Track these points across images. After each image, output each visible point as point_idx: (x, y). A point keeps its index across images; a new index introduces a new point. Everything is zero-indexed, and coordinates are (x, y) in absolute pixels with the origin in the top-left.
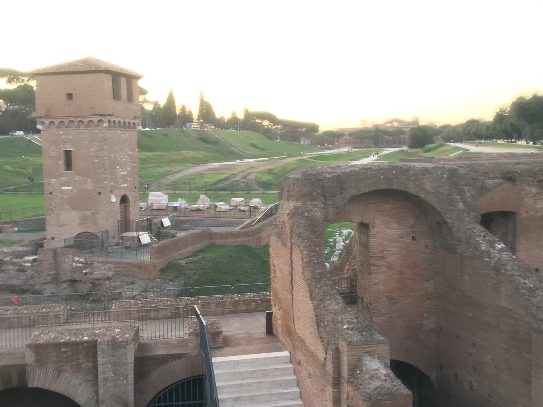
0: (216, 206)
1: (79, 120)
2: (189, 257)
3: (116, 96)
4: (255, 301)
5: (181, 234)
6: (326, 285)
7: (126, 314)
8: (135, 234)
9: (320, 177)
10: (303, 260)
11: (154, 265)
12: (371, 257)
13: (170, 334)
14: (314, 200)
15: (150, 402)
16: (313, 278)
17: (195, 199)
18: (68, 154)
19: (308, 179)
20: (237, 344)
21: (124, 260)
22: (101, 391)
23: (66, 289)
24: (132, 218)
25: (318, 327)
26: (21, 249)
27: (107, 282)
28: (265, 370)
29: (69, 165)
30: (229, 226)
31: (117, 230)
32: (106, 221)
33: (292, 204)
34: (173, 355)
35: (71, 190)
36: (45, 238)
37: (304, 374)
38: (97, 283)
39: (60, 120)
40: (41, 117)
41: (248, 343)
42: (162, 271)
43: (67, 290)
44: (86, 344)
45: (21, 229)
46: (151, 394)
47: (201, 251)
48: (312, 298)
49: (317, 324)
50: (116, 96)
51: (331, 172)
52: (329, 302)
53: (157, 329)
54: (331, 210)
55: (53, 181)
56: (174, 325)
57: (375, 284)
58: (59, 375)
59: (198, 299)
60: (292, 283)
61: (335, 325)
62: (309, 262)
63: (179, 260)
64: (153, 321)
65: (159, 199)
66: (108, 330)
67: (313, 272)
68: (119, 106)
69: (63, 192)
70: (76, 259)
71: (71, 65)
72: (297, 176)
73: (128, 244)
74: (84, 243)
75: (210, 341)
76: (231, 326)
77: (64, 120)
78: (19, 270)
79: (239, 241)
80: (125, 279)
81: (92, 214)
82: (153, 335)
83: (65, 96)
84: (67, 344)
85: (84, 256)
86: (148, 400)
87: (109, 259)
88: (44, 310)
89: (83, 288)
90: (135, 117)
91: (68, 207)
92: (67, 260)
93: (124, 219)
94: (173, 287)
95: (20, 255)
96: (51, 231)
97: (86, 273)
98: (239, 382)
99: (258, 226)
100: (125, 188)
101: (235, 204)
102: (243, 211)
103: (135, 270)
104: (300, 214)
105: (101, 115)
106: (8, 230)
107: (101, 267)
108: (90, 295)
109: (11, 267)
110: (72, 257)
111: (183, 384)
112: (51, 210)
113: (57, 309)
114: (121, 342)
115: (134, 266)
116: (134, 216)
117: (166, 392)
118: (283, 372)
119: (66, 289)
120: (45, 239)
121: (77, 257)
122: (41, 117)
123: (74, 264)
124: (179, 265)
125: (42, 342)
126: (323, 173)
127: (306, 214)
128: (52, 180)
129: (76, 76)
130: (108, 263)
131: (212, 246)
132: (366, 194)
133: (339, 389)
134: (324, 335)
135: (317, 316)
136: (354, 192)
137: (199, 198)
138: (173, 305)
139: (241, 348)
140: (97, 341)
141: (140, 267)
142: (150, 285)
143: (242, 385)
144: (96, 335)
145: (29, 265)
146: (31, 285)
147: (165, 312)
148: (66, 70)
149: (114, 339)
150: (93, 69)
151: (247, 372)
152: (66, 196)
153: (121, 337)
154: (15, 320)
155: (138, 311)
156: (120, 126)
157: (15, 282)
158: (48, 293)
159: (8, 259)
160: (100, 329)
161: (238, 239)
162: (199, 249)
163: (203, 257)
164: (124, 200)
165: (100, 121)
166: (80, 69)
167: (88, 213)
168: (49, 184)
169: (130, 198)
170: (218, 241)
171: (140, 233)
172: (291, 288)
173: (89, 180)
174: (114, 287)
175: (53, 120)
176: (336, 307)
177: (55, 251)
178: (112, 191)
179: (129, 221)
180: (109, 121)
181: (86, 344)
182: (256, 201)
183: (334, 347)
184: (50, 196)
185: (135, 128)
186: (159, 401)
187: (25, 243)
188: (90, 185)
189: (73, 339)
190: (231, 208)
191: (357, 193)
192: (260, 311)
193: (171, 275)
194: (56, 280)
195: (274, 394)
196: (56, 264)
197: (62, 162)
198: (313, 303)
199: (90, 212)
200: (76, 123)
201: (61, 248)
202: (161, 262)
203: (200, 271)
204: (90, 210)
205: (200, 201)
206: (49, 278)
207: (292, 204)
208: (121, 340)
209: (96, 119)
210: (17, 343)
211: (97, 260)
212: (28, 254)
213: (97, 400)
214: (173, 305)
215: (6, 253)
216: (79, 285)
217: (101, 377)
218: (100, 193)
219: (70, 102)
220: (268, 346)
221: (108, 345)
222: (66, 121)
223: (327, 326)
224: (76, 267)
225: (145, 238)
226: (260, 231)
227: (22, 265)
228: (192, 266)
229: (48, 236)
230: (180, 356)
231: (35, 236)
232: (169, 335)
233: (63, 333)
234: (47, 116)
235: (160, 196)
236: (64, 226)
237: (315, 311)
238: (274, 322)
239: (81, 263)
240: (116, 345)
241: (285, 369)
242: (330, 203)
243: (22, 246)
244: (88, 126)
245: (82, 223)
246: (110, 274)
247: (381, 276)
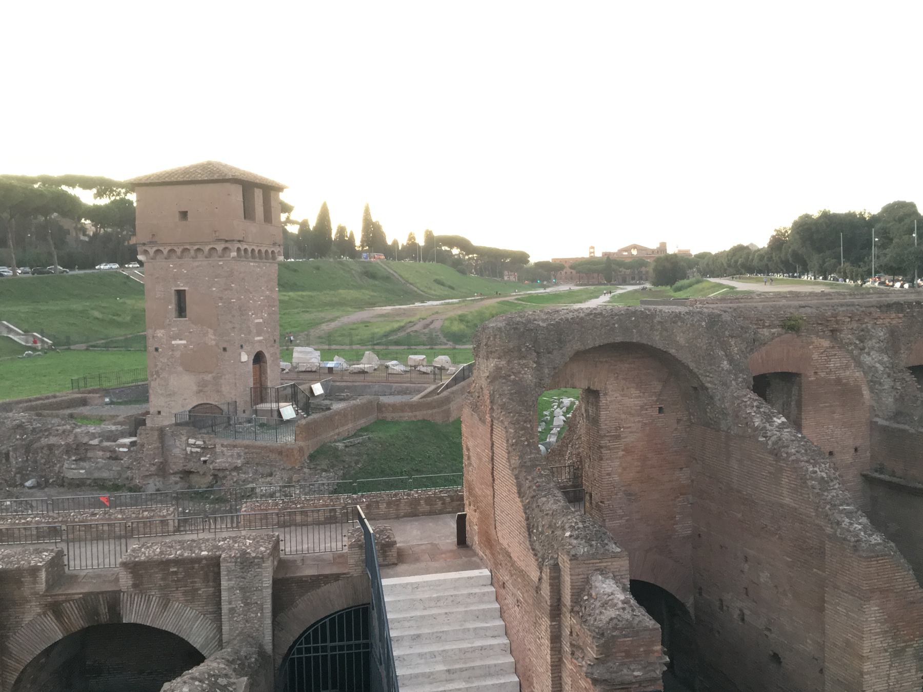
0: (387, 367)
1: (196, 247)
2: (349, 438)
3: (248, 214)
4: (441, 498)
5: (337, 406)
6: (541, 476)
7: (261, 519)
8: (274, 406)
9: (531, 326)
10: (508, 441)
11: (301, 450)
12: (602, 437)
13: (322, 546)
14: (524, 357)
15: (295, 643)
16: (522, 466)
17: (358, 358)
18: (180, 294)
19: (515, 329)
20: (417, 560)
21: (258, 443)
22: (225, 628)
23: (176, 483)
24: (269, 385)
25: (529, 535)
26: (113, 428)
27: (234, 474)
28: (456, 596)
29: (181, 311)
30: (405, 394)
31: (248, 399)
32: (234, 388)
33: (492, 363)
34: (326, 576)
35: (185, 346)
36: (148, 413)
37: (510, 600)
38: (221, 474)
39: (169, 248)
40: (144, 244)
41: (432, 558)
42: (312, 457)
43: (178, 486)
44: (204, 562)
45: (115, 400)
46: (295, 630)
47: (365, 429)
48: (520, 494)
49: (528, 531)
50: (248, 214)
51: (547, 319)
52: (544, 499)
53: (305, 539)
54: (546, 371)
55: (160, 333)
56: (328, 534)
57: (609, 474)
58: (165, 606)
59: (362, 496)
60: (492, 473)
61: (553, 532)
62: (516, 444)
63: (335, 441)
64: (299, 529)
65: (308, 357)
66: (235, 542)
67: (521, 457)
68: (253, 229)
69: (173, 348)
70: (191, 441)
71: (186, 171)
72: (500, 325)
73: (264, 419)
74: (201, 419)
75: (378, 556)
76: (408, 535)
77: (175, 248)
78: (110, 458)
79: (420, 415)
80: (260, 469)
81: (214, 378)
82: (299, 548)
83: (177, 215)
84: (177, 562)
85: (202, 437)
86: (292, 639)
87: (239, 442)
88: (146, 513)
89: (201, 483)
90: (274, 244)
91: (180, 369)
92: (178, 443)
93: (258, 385)
94: (325, 479)
95: (113, 437)
96: (156, 402)
97: (205, 462)
98: (418, 613)
99: (445, 393)
100: (260, 341)
101: (413, 364)
102: (424, 373)
103: (273, 456)
104: (504, 378)
105: (227, 241)
106: (96, 402)
107: (226, 453)
108: (211, 492)
109: (100, 453)
110: (184, 438)
111: (341, 617)
112: (157, 372)
113: (165, 512)
114: (254, 558)
115: (272, 450)
116: (273, 380)
117: (317, 629)
118: (482, 598)
119: (176, 483)
120: (148, 413)
121: (193, 438)
122: (144, 244)
123: (189, 449)
124: (336, 449)
125: (143, 558)
126: (535, 320)
127: (513, 377)
128: (158, 331)
129: (192, 186)
130: (235, 446)
131: (381, 423)
132: (595, 349)
133: (560, 621)
134: (537, 546)
135: (527, 519)
136: (578, 346)
137: (363, 355)
138: (327, 506)
139: (422, 565)
140: (220, 557)
141: (281, 452)
142: (295, 477)
143: (423, 617)
144: (218, 548)
145: (126, 450)
146: (127, 479)
147: (316, 515)
148: (179, 179)
149: (244, 553)
150: (216, 177)
151: (430, 599)
152: (178, 354)
153: (254, 552)
154: (106, 528)
155: (277, 514)
156: (253, 256)
157: (105, 475)
158: (151, 489)
159: (95, 442)
160: (224, 539)
161: (417, 413)
162: (364, 425)
163: (369, 438)
164: (259, 358)
165: (225, 249)
166: (199, 177)
167: (209, 377)
168: (153, 337)
169: (267, 355)
170: (389, 416)
171: (281, 404)
172: (491, 479)
173: (211, 331)
174: (244, 481)
175: (161, 248)
176: (555, 507)
177: (161, 431)
178: (242, 346)
179: (266, 388)
180: (239, 249)
181: (204, 562)
182: (442, 360)
183: (552, 562)
184: (155, 353)
185: (274, 258)
186: (308, 642)
187: (120, 419)
188: (211, 338)
189: (186, 554)
190: (408, 369)
191: (582, 348)
192: (449, 513)
193: (324, 464)
194: (162, 471)
195: (469, 630)
196: (163, 448)
197: (172, 307)
198: (522, 501)
199: (210, 375)
200: (192, 252)
201: (170, 426)
202: (310, 446)
203: (365, 456)
204: (211, 373)
205: (364, 360)
206: (153, 469)
207: (492, 363)
208: (254, 555)
209: (220, 247)
210: (107, 561)
211: (220, 443)
212: (123, 435)
213: (221, 640)
214: (327, 506)
215: (93, 433)
216: (194, 479)
217: (225, 607)
219: (184, 222)
220: (459, 561)
221: (236, 562)
222: (179, 251)
223: (542, 533)
224: (191, 452)
225: (288, 411)
226: (447, 400)
227: (115, 451)
228: (354, 450)
229: (152, 410)
230: (336, 577)
231: (134, 410)
232: (320, 547)
233: (172, 547)
234: (152, 243)
235: (309, 352)
236: (174, 395)
237: (525, 513)
238: (468, 528)
239: (198, 446)
240: (246, 562)
241: (484, 594)
242: (545, 362)
243: (115, 424)
244: (209, 255)
245: (200, 391)
246: (239, 462)
247: (617, 463)
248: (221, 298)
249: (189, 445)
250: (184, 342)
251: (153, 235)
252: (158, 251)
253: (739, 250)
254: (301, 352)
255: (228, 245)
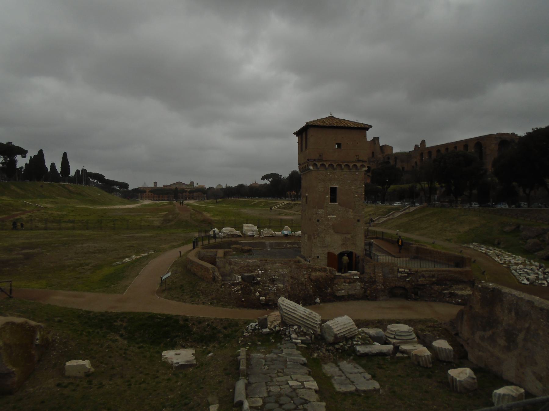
1: (345, 164)
35: (336, 218)
39: (330, 163)
123: (399, 274)
145: (358, 277)
152: (331, 223)
167: (349, 236)
168: (316, 214)
173: (351, 210)
175: (325, 163)
197: (328, 196)
218: (358, 221)
248: (357, 192)
249: (400, 272)
250: (335, 216)
251: (320, 155)
252: (323, 165)
253: (241, 186)
254: (248, 226)
255: (363, 164)
